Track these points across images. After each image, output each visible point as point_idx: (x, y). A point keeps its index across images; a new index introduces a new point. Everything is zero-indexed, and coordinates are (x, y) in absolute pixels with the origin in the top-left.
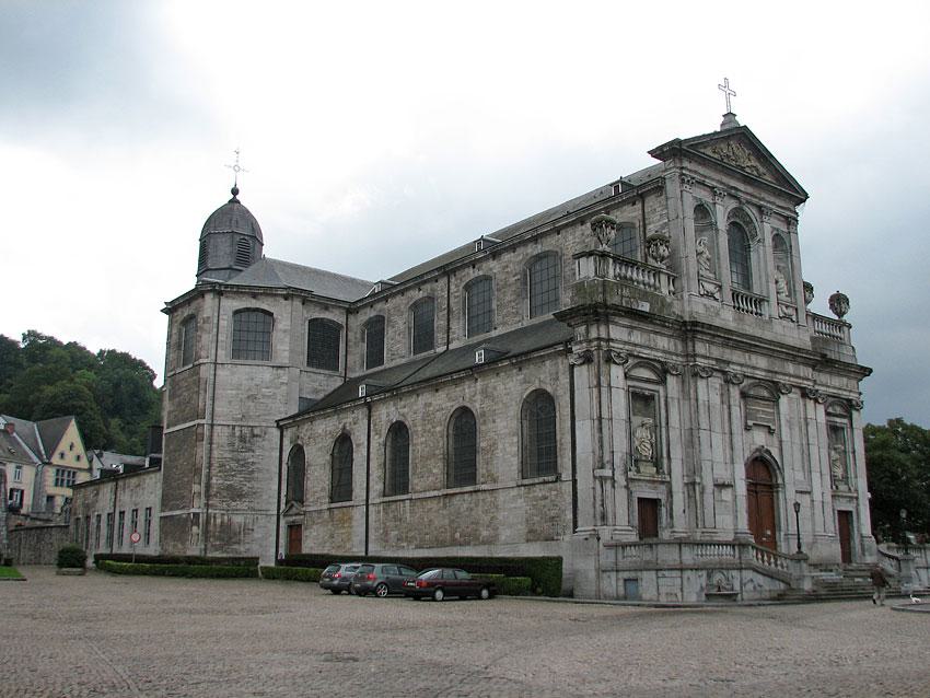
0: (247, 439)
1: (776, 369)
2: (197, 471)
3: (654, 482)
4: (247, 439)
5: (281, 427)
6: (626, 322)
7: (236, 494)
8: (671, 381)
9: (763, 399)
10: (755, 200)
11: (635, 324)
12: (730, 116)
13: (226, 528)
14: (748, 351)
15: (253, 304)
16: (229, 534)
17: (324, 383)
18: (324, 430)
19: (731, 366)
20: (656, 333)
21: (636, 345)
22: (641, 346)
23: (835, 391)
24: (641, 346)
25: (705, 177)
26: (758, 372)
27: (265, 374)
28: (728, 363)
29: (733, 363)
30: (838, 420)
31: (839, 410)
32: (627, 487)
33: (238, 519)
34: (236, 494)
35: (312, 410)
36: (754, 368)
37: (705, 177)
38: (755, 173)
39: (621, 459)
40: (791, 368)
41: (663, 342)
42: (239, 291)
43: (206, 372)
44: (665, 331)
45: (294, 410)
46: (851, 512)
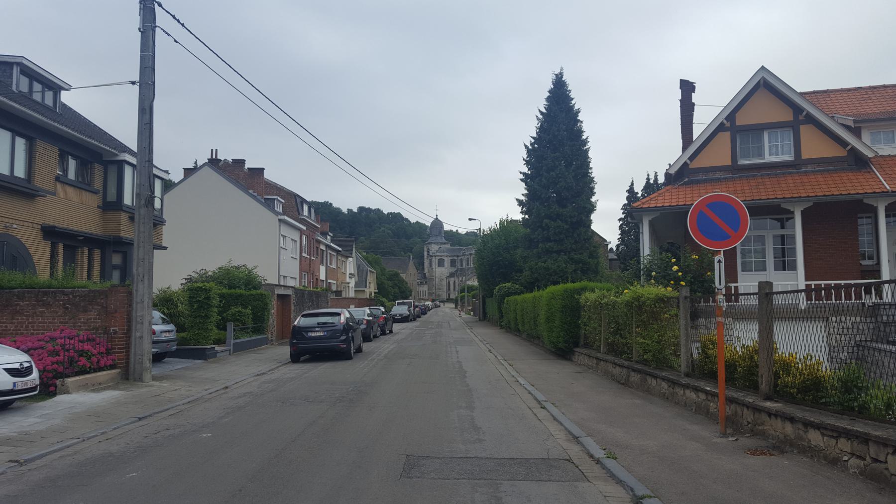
0: (441, 280)
2: (434, 285)
4: (441, 280)
5: (446, 277)
7: (440, 289)
13: (439, 295)
15: (440, 258)
16: (439, 295)
17: (453, 270)
18: (452, 280)
27: (443, 269)
33: (440, 293)
34: (440, 289)
35: (452, 275)
42: (438, 256)
43: (434, 269)
45: (448, 275)
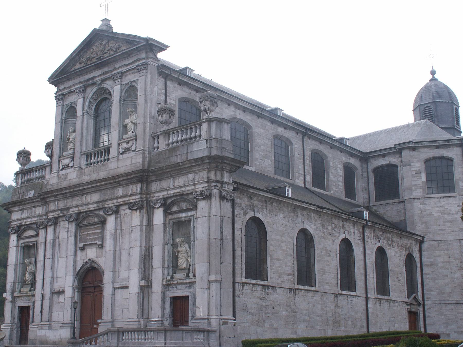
1: (107, 198)
3: (29, 296)
6: (16, 209)
8: (42, 232)
9: (94, 224)
10: (107, 76)
11: (21, 207)
12: (106, 21)
14: (83, 194)
19: (71, 210)
20: (34, 207)
21: (23, 219)
22: (26, 218)
23: (178, 190)
24: (26, 218)
25: (70, 87)
26: (91, 206)
28: (68, 209)
29: (72, 208)
30: (184, 215)
31: (184, 206)
32: (12, 302)
36: (87, 204)
37: (70, 87)
38: (112, 53)
39: (11, 286)
40: (120, 191)
41: (39, 210)
44: (37, 204)
46: (188, 297)
